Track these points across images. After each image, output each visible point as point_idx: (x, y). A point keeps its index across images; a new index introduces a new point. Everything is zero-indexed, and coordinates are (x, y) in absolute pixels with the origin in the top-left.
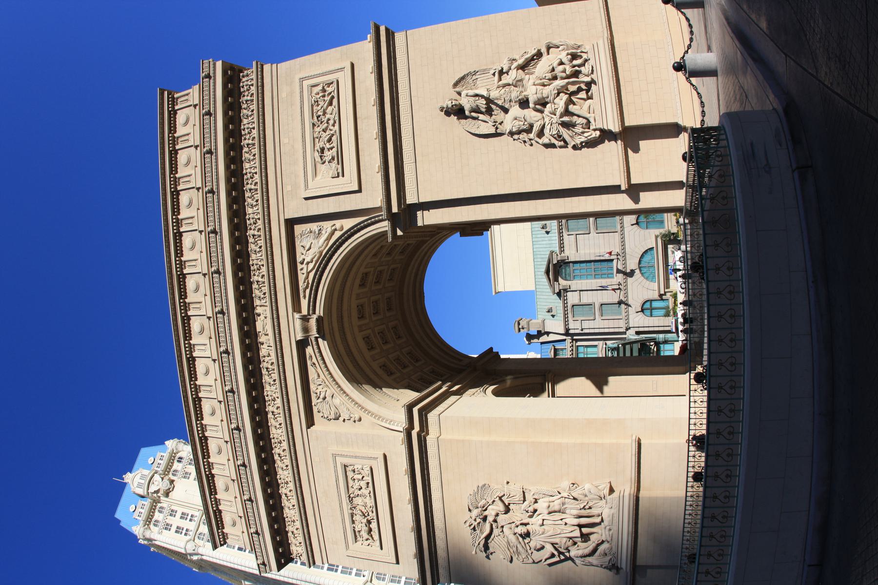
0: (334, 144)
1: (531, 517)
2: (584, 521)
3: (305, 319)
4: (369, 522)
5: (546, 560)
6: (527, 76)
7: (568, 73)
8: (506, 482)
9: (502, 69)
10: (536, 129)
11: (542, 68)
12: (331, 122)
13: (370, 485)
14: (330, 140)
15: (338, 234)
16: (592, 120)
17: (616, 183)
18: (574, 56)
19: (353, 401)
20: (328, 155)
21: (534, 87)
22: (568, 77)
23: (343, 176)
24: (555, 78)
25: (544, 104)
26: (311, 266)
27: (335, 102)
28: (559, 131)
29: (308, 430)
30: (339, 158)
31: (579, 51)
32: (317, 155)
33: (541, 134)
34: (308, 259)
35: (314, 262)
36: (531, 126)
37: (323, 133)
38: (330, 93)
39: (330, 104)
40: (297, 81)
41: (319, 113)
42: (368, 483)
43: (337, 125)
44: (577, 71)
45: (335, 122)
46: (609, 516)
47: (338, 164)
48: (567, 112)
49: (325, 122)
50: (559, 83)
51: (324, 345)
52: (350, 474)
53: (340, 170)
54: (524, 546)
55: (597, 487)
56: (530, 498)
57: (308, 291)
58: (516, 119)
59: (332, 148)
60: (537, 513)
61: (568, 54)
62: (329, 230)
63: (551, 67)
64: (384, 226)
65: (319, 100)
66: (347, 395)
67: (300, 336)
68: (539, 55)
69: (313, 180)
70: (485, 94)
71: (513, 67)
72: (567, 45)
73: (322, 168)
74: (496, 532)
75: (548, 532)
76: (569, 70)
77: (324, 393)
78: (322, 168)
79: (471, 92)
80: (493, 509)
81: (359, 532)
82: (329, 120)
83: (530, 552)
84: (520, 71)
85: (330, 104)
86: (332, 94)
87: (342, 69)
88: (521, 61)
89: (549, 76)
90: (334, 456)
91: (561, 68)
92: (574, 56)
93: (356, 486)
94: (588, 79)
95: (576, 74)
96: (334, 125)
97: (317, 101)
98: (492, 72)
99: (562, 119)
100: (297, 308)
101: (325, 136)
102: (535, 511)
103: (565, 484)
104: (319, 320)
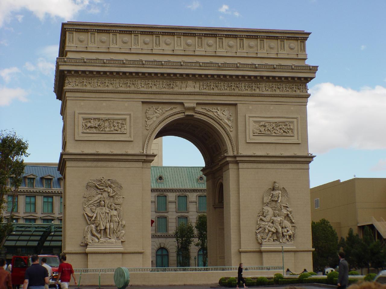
0: (267, 132)
1: (108, 207)
2: (108, 231)
3: (193, 109)
4: (96, 128)
5: (86, 214)
6: (284, 217)
7: (284, 233)
8: (124, 197)
9: (288, 208)
10: (264, 218)
11: (287, 223)
12: (276, 132)
13: (116, 132)
17: (242, 247)
18: (290, 236)
19: (156, 128)
20: (262, 129)
21: (280, 220)
22: (282, 233)
24: (282, 228)
25: (272, 223)
26: (215, 114)
27: (284, 134)
30: (261, 134)
31: (292, 238)
32: (262, 124)
34: (219, 113)
35: (217, 115)
36: (265, 217)
38: (288, 132)
39: (284, 132)
40: (297, 116)
41: (281, 126)
43: (274, 134)
44: (284, 236)
46: (112, 241)
48: (269, 231)
50: (280, 230)
51: (181, 116)
53: (255, 134)
54: (92, 204)
55: (123, 236)
56: (117, 207)
57: (205, 111)
59: (265, 131)
60: (110, 210)
61: (291, 234)
62: (230, 125)
63: (287, 227)
64: (230, 153)
65: (287, 126)
66: (158, 125)
67: (186, 105)
68: (292, 223)
70: (279, 201)
72: (294, 234)
73: (257, 126)
74: (98, 191)
75: (103, 215)
76: (284, 233)
77: (159, 113)
78: (257, 126)
79: (280, 195)
80: (111, 190)
81: (90, 122)
82: (277, 130)
83: (89, 206)
84: (286, 215)
85: (284, 132)
86: (288, 133)
87: (298, 139)
88: (290, 216)
89: (283, 226)
90: (130, 115)
91: (286, 231)
92: (290, 236)
93: (115, 124)
94: (281, 241)
95: (283, 236)
96: (274, 133)
97: (286, 125)
98: (287, 204)
99: (267, 229)
100: (198, 104)
102: (112, 210)
103: (124, 223)
104: (193, 116)
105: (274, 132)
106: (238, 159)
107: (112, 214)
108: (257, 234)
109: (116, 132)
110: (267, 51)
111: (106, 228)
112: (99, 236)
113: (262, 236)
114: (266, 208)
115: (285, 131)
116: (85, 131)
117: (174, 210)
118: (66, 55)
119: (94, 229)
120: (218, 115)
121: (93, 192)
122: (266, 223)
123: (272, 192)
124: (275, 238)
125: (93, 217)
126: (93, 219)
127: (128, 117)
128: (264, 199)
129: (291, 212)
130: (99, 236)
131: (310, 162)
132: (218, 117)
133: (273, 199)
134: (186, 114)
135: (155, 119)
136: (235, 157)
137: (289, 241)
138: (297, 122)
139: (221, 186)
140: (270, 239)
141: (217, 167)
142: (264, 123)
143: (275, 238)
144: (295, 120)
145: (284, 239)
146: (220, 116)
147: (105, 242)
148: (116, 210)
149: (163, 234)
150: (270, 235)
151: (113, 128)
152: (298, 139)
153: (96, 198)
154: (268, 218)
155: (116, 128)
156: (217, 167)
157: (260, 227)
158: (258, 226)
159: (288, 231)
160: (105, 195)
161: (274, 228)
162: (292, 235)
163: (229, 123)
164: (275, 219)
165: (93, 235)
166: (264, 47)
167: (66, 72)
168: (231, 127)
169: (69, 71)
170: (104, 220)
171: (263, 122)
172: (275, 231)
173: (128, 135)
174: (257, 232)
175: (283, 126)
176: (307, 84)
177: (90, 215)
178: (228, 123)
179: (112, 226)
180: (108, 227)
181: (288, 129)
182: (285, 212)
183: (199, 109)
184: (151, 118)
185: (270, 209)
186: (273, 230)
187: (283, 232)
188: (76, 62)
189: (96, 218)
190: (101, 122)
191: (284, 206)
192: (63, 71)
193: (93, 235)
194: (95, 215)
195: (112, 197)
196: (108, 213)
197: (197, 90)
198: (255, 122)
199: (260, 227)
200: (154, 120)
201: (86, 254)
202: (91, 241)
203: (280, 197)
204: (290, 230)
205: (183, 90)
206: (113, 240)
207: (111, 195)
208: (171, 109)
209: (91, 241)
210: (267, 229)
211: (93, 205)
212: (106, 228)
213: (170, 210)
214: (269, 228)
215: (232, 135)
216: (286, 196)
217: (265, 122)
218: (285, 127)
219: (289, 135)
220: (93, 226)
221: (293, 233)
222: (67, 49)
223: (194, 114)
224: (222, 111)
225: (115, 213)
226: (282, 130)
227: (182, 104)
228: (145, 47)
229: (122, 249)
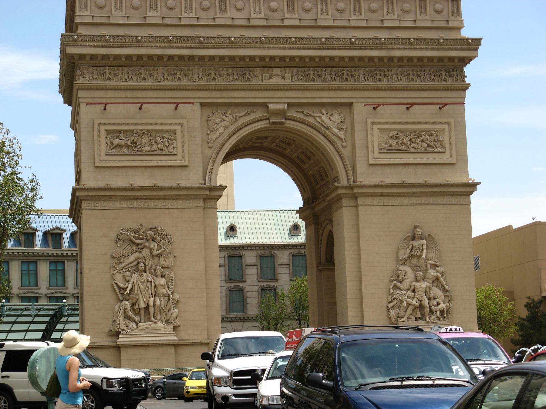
2: (151, 310)
3: (281, 113)
4: (128, 146)
5: (116, 284)
6: (431, 282)
8: (176, 255)
9: (438, 267)
10: (399, 285)
11: (437, 292)
13: (161, 153)
14: (403, 144)
15: (339, 143)
16: (403, 320)
18: (442, 312)
20: (394, 142)
22: (430, 307)
23: (380, 153)
24: (429, 299)
25: (414, 291)
26: (318, 119)
27: (429, 149)
28: (398, 299)
29: (199, 103)
30: (391, 150)
31: (445, 315)
33: (396, 287)
34: (324, 117)
36: (401, 282)
37: (409, 139)
38: (436, 146)
39: (429, 146)
40: (449, 120)
41: (423, 137)
42: (162, 150)
43: (413, 150)
45: (415, 149)
46: (159, 327)
47: (388, 150)
48: (409, 304)
49: (417, 141)
50: (426, 302)
52: (167, 135)
53: (383, 151)
54: (126, 267)
55: (176, 318)
57: (300, 116)
58: (406, 273)
59: (398, 145)
60: (155, 277)
62: (342, 137)
63: (436, 297)
64: (344, 181)
65: (433, 137)
68: (444, 290)
69: (378, 129)
70: (424, 256)
71: (438, 273)
72: (449, 308)
73: (385, 137)
76: (433, 307)
77: (227, 120)
79: (425, 247)
80: (154, 246)
82: (418, 144)
83: (121, 271)
84: (435, 278)
85: (429, 146)
86: (435, 148)
87: (451, 157)
88: (441, 279)
89: (431, 295)
90: (181, 124)
91: (435, 303)
92: (442, 312)
93: (160, 141)
94: (428, 320)
95: (431, 311)
96: (413, 147)
97: (431, 135)
98: (436, 260)
99: (405, 301)
100: (289, 105)
101: (406, 140)
102: (157, 276)
103: (177, 296)
104: (282, 123)
105: (412, 146)
106: (356, 191)
107: (157, 283)
108: (390, 310)
109: (161, 153)
110: (398, 16)
111: (148, 306)
112: (137, 319)
113: (397, 312)
114: (403, 268)
115: (431, 144)
116: (110, 152)
117: (255, 277)
118: (77, 30)
119: (129, 308)
120: (323, 121)
121: (127, 249)
122: (404, 292)
123: (412, 242)
124: (419, 315)
125: (127, 288)
126: (128, 291)
127: (178, 128)
128: (400, 254)
129: (442, 274)
130: (137, 319)
131: (472, 193)
132: (322, 125)
133: (413, 253)
134: (271, 121)
135: (221, 130)
136: (352, 188)
137: (441, 319)
138: (450, 129)
139: (331, 235)
140: (411, 317)
141: (323, 205)
142: (395, 133)
143: (419, 315)
144: (446, 126)
145: (433, 317)
146: (325, 124)
147: (147, 328)
148: (163, 276)
149: (239, 316)
150: (410, 310)
151: (155, 146)
152: (451, 157)
153: (132, 259)
154: (406, 284)
155: (160, 146)
156: (323, 205)
157: (394, 299)
158: (390, 296)
159: (438, 304)
160: (146, 253)
161: (415, 299)
162: (445, 310)
163: (341, 134)
164: (417, 284)
165: (128, 318)
166: (393, 10)
167: (77, 59)
168: (344, 140)
169: (82, 57)
170: (144, 293)
171: (394, 132)
172: (417, 304)
173: (180, 157)
174: (390, 307)
175: (427, 137)
176: (464, 68)
177: (121, 285)
178: (339, 134)
179: (158, 303)
180: (151, 303)
181: (435, 141)
182: (432, 273)
183: (293, 113)
184: (215, 129)
185: (408, 270)
186: (415, 302)
187: (431, 304)
188: (93, 40)
189: (132, 289)
190: (134, 137)
191: (430, 264)
192: (72, 56)
193: (128, 318)
194: (130, 286)
195: (157, 255)
196: (151, 282)
197: (288, 82)
198: (381, 130)
199: (394, 299)
200: (221, 131)
201: (118, 348)
202: (125, 328)
203: (425, 251)
204: (442, 303)
205: (266, 83)
206: (160, 325)
207: (156, 253)
208: (248, 114)
209: (125, 328)
210: (406, 301)
211: (126, 270)
212: (148, 306)
213: (248, 277)
214: (408, 300)
215: (346, 152)
216: (434, 248)
217: (398, 131)
218: (430, 139)
219: (436, 150)
220: (127, 303)
221: (446, 306)
222: (77, 20)
223: (284, 121)
224: (328, 115)
225: (162, 281)
226: (426, 143)
227: (265, 105)
228: (203, 14)
229: (175, 338)
